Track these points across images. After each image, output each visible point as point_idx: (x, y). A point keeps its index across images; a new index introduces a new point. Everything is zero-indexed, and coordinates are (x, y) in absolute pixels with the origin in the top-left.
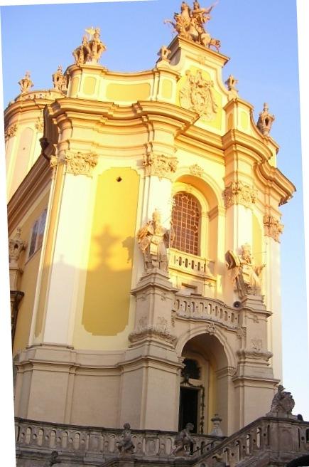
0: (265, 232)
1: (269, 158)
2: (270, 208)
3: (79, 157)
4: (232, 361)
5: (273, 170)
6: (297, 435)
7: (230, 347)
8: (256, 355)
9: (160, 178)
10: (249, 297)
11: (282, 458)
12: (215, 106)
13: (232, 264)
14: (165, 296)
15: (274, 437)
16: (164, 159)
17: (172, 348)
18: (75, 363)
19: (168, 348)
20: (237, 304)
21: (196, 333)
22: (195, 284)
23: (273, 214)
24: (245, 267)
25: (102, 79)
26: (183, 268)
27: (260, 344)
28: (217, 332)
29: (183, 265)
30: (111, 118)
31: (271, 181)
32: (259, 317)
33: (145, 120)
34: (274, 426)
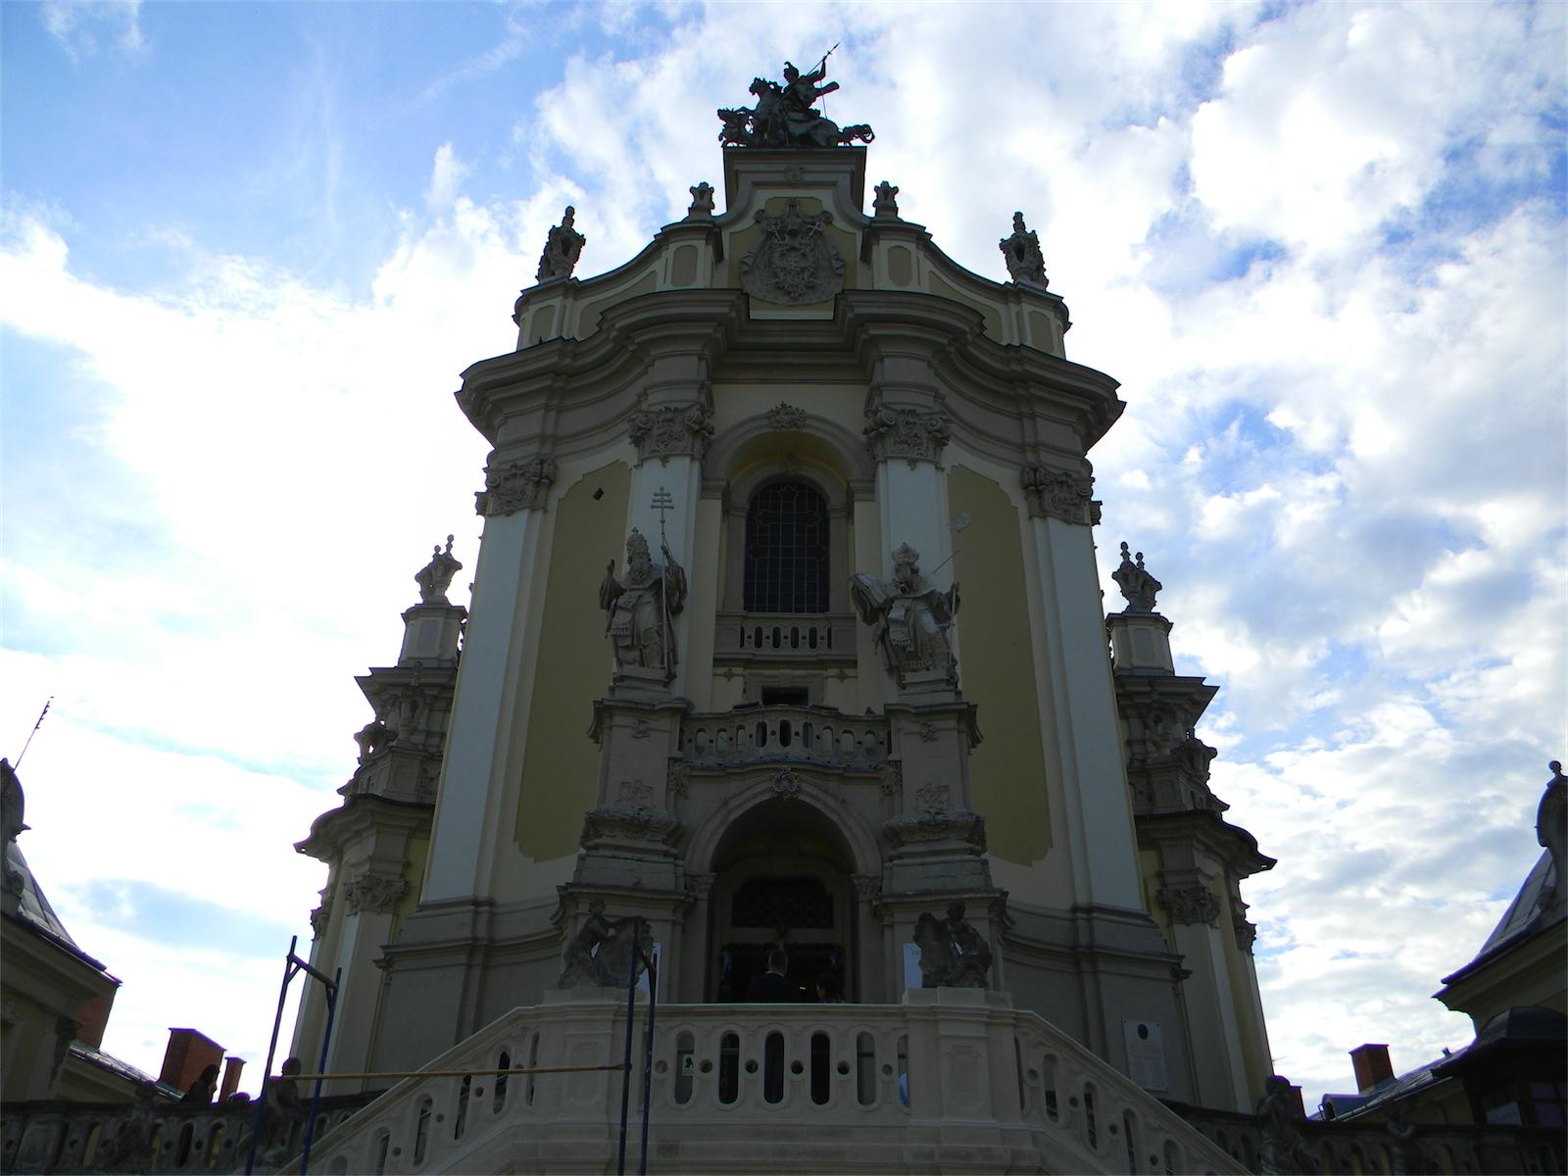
1: (983, 328)
2: (1036, 447)
4: (866, 859)
5: (1012, 354)
8: (934, 828)
9: (665, 460)
12: (835, 264)
13: (869, 608)
14: (643, 727)
16: (669, 415)
17: (666, 854)
18: (475, 939)
19: (647, 857)
21: (741, 805)
23: (1046, 458)
24: (896, 604)
25: (570, 300)
26: (767, 651)
29: (767, 644)
30: (572, 374)
31: (1026, 382)
32: (939, 724)
33: (631, 348)
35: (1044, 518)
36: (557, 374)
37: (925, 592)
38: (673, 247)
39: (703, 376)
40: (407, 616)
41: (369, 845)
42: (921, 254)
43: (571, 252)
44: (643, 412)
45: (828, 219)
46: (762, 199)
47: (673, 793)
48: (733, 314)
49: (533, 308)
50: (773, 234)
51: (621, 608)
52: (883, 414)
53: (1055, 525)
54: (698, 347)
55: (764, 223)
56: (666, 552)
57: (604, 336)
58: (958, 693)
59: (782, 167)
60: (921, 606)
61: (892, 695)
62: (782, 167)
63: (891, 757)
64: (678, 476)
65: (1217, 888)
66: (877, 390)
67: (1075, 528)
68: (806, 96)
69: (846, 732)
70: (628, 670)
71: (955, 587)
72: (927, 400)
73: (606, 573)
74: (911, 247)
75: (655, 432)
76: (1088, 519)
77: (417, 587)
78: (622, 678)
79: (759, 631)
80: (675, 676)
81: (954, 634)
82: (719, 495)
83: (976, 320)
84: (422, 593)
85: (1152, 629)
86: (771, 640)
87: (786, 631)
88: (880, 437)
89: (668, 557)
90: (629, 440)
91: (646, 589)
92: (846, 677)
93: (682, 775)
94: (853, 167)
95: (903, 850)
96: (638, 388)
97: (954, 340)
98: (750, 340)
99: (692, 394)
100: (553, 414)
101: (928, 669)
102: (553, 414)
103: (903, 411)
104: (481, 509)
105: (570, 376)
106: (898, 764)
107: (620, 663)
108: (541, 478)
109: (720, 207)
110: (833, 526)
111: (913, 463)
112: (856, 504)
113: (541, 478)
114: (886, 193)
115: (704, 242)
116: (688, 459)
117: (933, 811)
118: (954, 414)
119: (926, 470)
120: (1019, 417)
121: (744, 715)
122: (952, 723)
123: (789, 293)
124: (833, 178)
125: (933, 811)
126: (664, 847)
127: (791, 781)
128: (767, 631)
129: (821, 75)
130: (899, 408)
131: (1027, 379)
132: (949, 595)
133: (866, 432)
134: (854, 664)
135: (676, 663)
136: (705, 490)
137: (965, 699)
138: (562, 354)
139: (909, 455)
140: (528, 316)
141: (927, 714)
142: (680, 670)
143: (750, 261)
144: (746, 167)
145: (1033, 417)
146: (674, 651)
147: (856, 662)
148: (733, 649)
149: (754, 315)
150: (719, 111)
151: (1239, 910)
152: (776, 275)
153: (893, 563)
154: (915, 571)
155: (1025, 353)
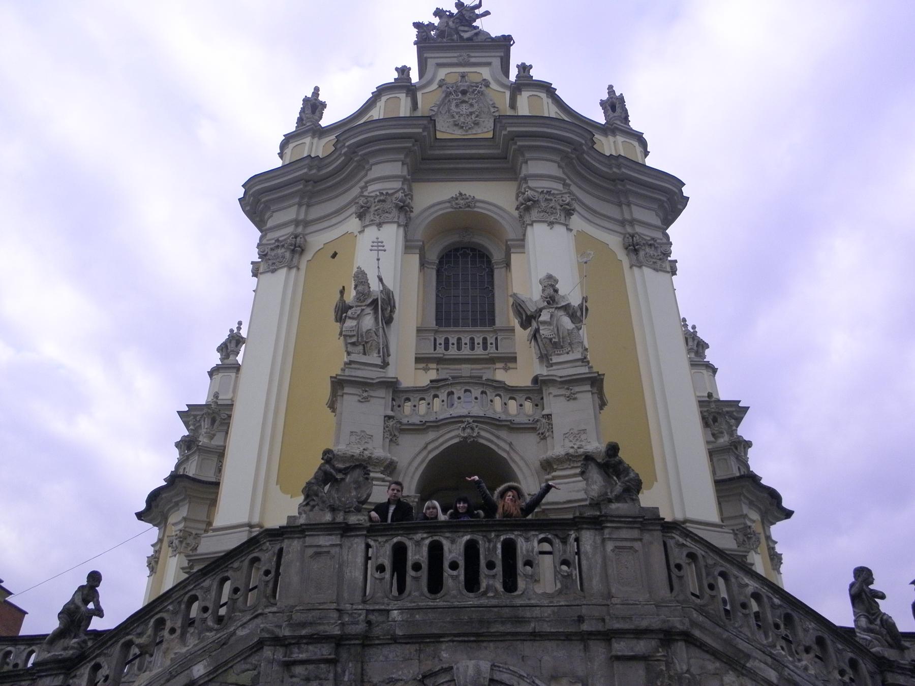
0: (630, 261)
2: (632, 222)
3: (278, 247)
5: (613, 162)
6: (360, 560)
7: (522, 458)
9: (379, 225)
10: (555, 359)
11: (291, 626)
12: (492, 110)
15: (291, 574)
16: (382, 198)
17: (383, 480)
20: (536, 380)
21: (437, 447)
22: (476, 373)
23: (639, 229)
24: (544, 312)
26: (453, 352)
27: (583, 437)
28: (483, 433)
31: (622, 181)
32: (577, 389)
34: (293, 547)
35: (640, 267)
36: (307, 181)
37: (563, 304)
38: (384, 99)
39: (405, 173)
40: (211, 374)
41: (183, 512)
42: (550, 101)
43: (317, 113)
44: (364, 196)
45: (487, 84)
46: (442, 73)
47: (388, 440)
48: (425, 134)
49: (291, 146)
50: (451, 93)
51: (350, 318)
52: (529, 193)
53: (647, 271)
54: (402, 156)
55: (444, 88)
56: (381, 280)
57: (337, 154)
58: (591, 368)
59: (455, 55)
60: (561, 313)
61: (541, 370)
62: (455, 55)
63: (545, 412)
64: (391, 235)
65: (757, 527)
66: (525, 179)
67: (661, 275)
68: (470, 17)
69: (511, 398)
70: (354, 357)
71: (585, 299)
72: (560, 187)
73: (339, 296)
74: (543, 95)
75: (372, 209)
76: (669, 269)
77: (219, 355)
78: (351, 362)
79: (447, 340)
80: (388, 364)
81: (584, 332)
82: (418, 251)
83: (589, 137)
84: (221, 359)
85: (705, 372)
86: (455, 346)
87: (466, 339)
88: (528, 209)
89: (382, 283)
90: (354, 215)
91: (368, 305)
92: (510, 368)
93: (396, 429)
94: (502, 54)
95: (554, 474)
96: (362, 184)
97: (575, 149)
98: (437, 152)
99: (397, 185)
100: (304, 208)
101: (568, 353)
102: (304, 208)
103: (542, 192)
104: (255, 273)
105: (315, 182)
106: (548, 416)
107: (349, 354)
108: (295, 247)
109: (414, 77)
110: (496, 272)
111: (551, 224)
112: (513, 256)
113: (295, 247)
114: (524, 69)
115: (404, 95)
116: (395, 226)
117: (576, 447)
118: (574, 195)
119: (560, 230)
120: (620, 205)
121: (438, 388)
122: (588, 388)
123: (462, 127)
124: (489, 60)
125: (576, 447)
126: (382, 476)
127: (472, 429)
128: (453, 340)
129: (479, 6)
130: (540, 190)
131: (623, 179)
132: (581, 307)
133: (517, 209)
134: (514, 359)
135: (389, 355)
136: (408, 247)
137: (595, 370)
138: (310, 168)
139: (548, 219)
140: (288, 151)
141: (570, 382)
142: (391, 360)
143: (435, 109)
144: (433, 55)
145: (629, 205)
146: (387, 346)
147: (516, 358)
148: (428, 350)
149: (439, 135)
150: (414, 24)
151: (771, 545)
152: (453, 117)
153: (541, 287)
154: (556, 291)
155: (621, 160)
